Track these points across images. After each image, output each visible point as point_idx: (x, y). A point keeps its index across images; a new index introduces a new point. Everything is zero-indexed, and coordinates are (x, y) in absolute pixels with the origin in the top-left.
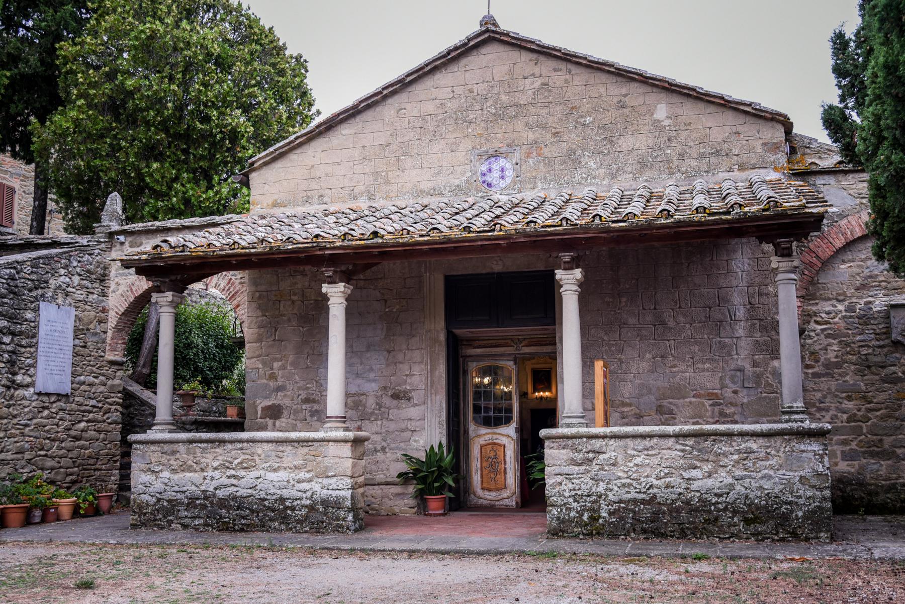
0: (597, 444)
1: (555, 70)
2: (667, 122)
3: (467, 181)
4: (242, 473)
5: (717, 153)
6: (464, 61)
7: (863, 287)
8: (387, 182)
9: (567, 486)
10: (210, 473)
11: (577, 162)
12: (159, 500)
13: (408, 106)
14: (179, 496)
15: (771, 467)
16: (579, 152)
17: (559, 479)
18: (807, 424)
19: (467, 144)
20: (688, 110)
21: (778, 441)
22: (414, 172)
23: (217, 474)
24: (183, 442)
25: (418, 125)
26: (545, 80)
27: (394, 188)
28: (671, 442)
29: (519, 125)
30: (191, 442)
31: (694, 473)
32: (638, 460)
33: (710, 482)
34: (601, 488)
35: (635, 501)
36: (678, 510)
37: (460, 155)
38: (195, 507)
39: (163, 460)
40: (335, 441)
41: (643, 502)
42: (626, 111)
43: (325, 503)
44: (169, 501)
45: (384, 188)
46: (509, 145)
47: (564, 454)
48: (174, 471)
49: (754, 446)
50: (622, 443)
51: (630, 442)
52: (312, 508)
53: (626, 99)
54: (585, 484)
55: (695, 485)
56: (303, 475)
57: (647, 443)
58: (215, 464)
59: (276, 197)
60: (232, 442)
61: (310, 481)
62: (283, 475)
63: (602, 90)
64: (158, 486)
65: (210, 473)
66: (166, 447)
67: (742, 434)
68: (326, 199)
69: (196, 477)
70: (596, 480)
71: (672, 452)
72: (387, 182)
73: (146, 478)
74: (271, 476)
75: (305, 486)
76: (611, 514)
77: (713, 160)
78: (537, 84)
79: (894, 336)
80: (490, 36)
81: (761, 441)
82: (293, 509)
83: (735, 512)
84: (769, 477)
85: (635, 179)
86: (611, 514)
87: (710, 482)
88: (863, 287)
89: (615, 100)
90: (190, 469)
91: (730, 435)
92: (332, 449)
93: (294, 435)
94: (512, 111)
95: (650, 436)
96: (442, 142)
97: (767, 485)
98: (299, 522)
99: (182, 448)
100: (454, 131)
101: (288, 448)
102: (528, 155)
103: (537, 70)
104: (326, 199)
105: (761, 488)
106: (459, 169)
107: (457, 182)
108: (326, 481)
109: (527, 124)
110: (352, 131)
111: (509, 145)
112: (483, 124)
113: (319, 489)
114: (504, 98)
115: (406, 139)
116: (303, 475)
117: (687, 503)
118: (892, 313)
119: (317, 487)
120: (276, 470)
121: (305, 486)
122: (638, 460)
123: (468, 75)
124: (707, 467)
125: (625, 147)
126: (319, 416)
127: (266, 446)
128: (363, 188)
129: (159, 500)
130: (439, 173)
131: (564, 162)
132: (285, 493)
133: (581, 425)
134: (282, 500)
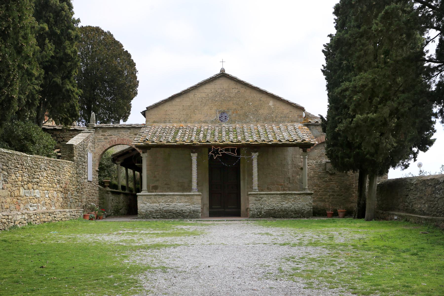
0: (262, 196)
1: (242, 87)
2: (272, 107)
3: (215, 119)
4: (171, 203)
5: (285, 117)
6: (214, 81)
7: (320, 156)
8: (191, 118)
9: (254, 206)
10: (161, 204)
11: (247, 116)
12: (146, 211)
13: (197, 94)
14: (152, 210)
15: (300, 202)
16: (248, 113)
17: (253, 204)
18: (308, 192)
19: (215, 108)
20: (278, 104)
21: (302, 196)
22: (199, 115)
23: (163, 204)
24: (153, 195)
25: (200, 100)
26: (239, 90)
27: (193, 119)
28: (278, 196)
29: (231, 103)
30: (155, 195)
31: (283, 203)
32: (271, 200)
33: (287, 205)
34: (262, 207)
35: (270, 209)
36: (280, 211)
37: (213, 111)
38: (157, 213)
39: (147, 200)
40: (196, 195)
41: (272, 210)
42: (261, 102)
43: (194, 211)
44: (150, 211)
45: (190, 119)
46: (228, 109)
47: (254, 198)
48: (151, 203)
49: (297, 197)
50: (267, 196)
51: (269, 196)
52: (190, 212)
53: (262, 98)
54: (259, 206)
55: (284, 206)
56: (187, 204)
57: (273, 196)
58: (163, 201)
59: (154, 119)
60: (167, 195)
61: (189, 205)
62: (182, 204)
63: (255, 95)
64: (146, 207)
65: (161, 204)
66: (148, 197)
67: (295, 194)
68: (171, 121)
69: (157, 205)
70: (261, 205)
71: (279, 198)
72: (191, 118)
73: (142, 205)
74: (179, 204)
75: (188, 207)
76: (264, 212)
77: (285, 119)
78: (236, 91)
79: (327, 170)
80: (223, 75)
81: (298, 196)
82: (185, 213)
83: (292, 212)
84: (300, 204)
85: (263, 123)
86: (264, 212)
87: (287, 205)
88: (320, 156)
89: (259, 98)
90: (155, 203)
91: (292, 194)
92: (195, 197)
93: (185, 193)
94: (229, 99)
95: (274, 194)
96: (208, 106)
97: (299, 205)
98: (187, 216)
99: (153, 197)
100: (211, 103)
101: (183, 197)
102: (233, 113)
103: (236, 87)
104: (171, 121)
105: (298, 206)
106: (213, 115)
107: (212, 119)
108: (194, 205)
109: (233, 103)
110: (179, 100)
111: (228, 109)
112: (220, 102)
113: (192, 207)
114: (226, 94)
115: (197, 104)
116: (187, 204)
117: (282, 210)
118: (327, 164)
119: (192, 207)
120: (180, 203)
121: (188, 207)
122: (271, 200)
123: (216, 86)
124: (286, 201)
125: (260, 113)
126: (189, 189)
127: (177, 196)
128: (183, 119)
129: (146, 211)
130: (206, 116)
131: (244, 116)
132: (183, 209)
133: (257, 191)
134: (182, 210)
